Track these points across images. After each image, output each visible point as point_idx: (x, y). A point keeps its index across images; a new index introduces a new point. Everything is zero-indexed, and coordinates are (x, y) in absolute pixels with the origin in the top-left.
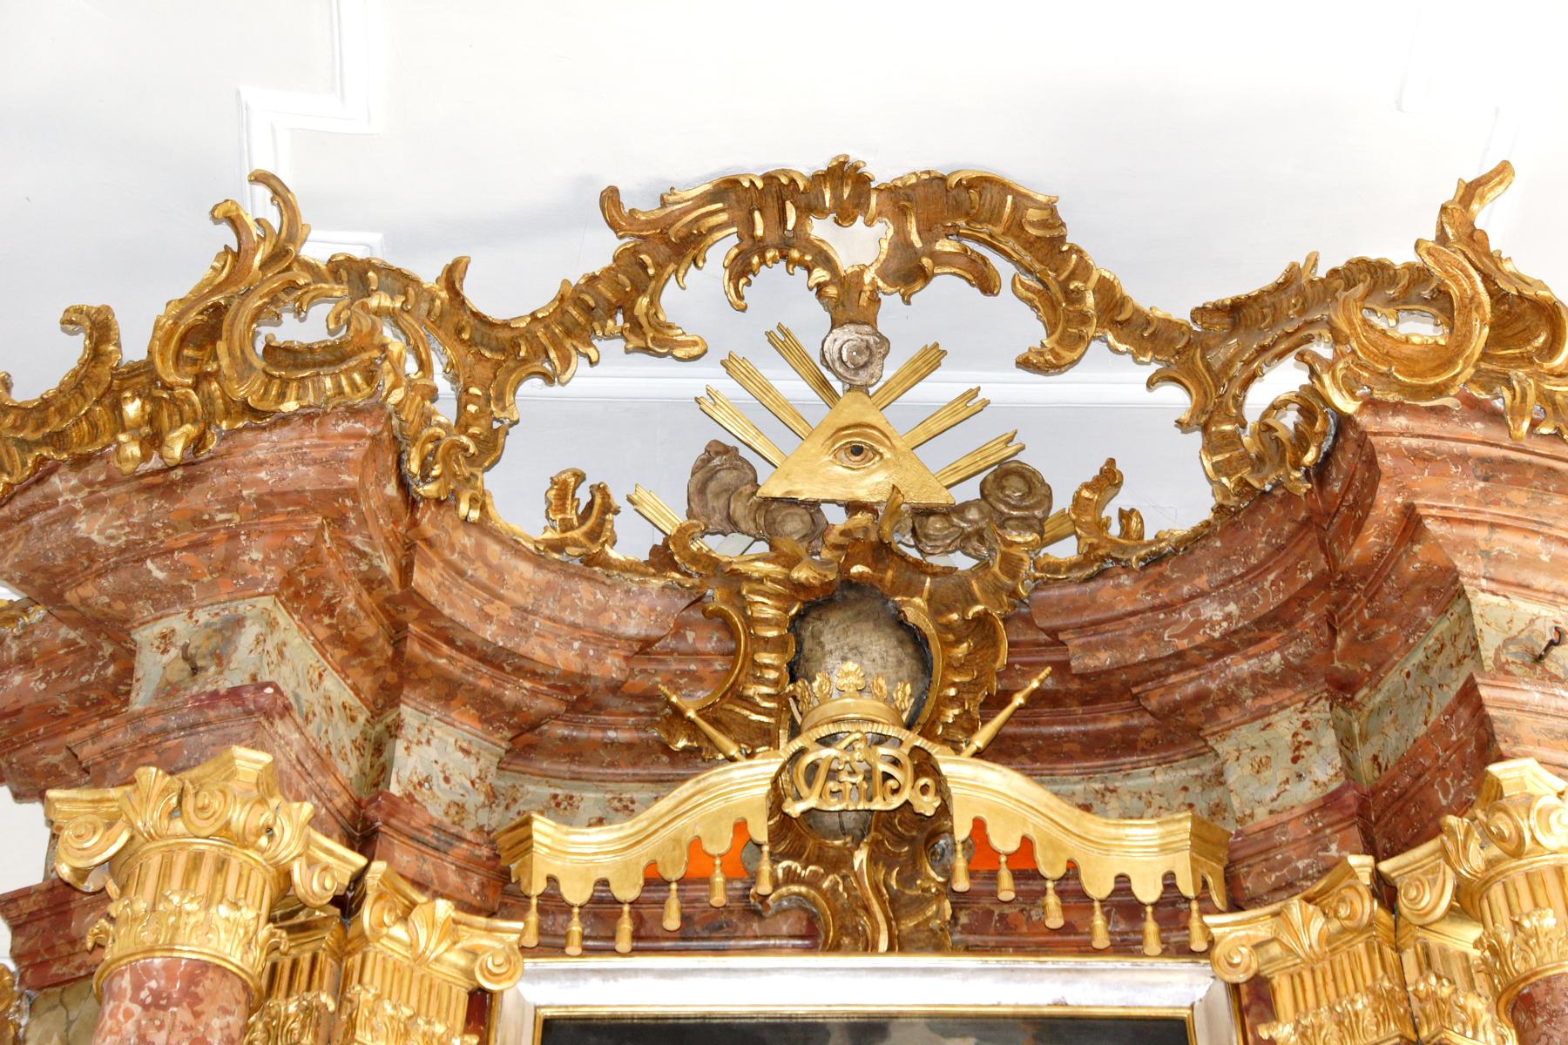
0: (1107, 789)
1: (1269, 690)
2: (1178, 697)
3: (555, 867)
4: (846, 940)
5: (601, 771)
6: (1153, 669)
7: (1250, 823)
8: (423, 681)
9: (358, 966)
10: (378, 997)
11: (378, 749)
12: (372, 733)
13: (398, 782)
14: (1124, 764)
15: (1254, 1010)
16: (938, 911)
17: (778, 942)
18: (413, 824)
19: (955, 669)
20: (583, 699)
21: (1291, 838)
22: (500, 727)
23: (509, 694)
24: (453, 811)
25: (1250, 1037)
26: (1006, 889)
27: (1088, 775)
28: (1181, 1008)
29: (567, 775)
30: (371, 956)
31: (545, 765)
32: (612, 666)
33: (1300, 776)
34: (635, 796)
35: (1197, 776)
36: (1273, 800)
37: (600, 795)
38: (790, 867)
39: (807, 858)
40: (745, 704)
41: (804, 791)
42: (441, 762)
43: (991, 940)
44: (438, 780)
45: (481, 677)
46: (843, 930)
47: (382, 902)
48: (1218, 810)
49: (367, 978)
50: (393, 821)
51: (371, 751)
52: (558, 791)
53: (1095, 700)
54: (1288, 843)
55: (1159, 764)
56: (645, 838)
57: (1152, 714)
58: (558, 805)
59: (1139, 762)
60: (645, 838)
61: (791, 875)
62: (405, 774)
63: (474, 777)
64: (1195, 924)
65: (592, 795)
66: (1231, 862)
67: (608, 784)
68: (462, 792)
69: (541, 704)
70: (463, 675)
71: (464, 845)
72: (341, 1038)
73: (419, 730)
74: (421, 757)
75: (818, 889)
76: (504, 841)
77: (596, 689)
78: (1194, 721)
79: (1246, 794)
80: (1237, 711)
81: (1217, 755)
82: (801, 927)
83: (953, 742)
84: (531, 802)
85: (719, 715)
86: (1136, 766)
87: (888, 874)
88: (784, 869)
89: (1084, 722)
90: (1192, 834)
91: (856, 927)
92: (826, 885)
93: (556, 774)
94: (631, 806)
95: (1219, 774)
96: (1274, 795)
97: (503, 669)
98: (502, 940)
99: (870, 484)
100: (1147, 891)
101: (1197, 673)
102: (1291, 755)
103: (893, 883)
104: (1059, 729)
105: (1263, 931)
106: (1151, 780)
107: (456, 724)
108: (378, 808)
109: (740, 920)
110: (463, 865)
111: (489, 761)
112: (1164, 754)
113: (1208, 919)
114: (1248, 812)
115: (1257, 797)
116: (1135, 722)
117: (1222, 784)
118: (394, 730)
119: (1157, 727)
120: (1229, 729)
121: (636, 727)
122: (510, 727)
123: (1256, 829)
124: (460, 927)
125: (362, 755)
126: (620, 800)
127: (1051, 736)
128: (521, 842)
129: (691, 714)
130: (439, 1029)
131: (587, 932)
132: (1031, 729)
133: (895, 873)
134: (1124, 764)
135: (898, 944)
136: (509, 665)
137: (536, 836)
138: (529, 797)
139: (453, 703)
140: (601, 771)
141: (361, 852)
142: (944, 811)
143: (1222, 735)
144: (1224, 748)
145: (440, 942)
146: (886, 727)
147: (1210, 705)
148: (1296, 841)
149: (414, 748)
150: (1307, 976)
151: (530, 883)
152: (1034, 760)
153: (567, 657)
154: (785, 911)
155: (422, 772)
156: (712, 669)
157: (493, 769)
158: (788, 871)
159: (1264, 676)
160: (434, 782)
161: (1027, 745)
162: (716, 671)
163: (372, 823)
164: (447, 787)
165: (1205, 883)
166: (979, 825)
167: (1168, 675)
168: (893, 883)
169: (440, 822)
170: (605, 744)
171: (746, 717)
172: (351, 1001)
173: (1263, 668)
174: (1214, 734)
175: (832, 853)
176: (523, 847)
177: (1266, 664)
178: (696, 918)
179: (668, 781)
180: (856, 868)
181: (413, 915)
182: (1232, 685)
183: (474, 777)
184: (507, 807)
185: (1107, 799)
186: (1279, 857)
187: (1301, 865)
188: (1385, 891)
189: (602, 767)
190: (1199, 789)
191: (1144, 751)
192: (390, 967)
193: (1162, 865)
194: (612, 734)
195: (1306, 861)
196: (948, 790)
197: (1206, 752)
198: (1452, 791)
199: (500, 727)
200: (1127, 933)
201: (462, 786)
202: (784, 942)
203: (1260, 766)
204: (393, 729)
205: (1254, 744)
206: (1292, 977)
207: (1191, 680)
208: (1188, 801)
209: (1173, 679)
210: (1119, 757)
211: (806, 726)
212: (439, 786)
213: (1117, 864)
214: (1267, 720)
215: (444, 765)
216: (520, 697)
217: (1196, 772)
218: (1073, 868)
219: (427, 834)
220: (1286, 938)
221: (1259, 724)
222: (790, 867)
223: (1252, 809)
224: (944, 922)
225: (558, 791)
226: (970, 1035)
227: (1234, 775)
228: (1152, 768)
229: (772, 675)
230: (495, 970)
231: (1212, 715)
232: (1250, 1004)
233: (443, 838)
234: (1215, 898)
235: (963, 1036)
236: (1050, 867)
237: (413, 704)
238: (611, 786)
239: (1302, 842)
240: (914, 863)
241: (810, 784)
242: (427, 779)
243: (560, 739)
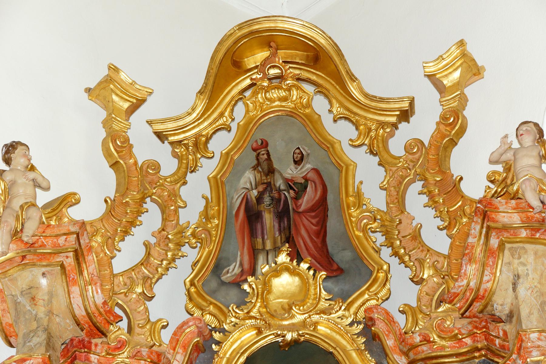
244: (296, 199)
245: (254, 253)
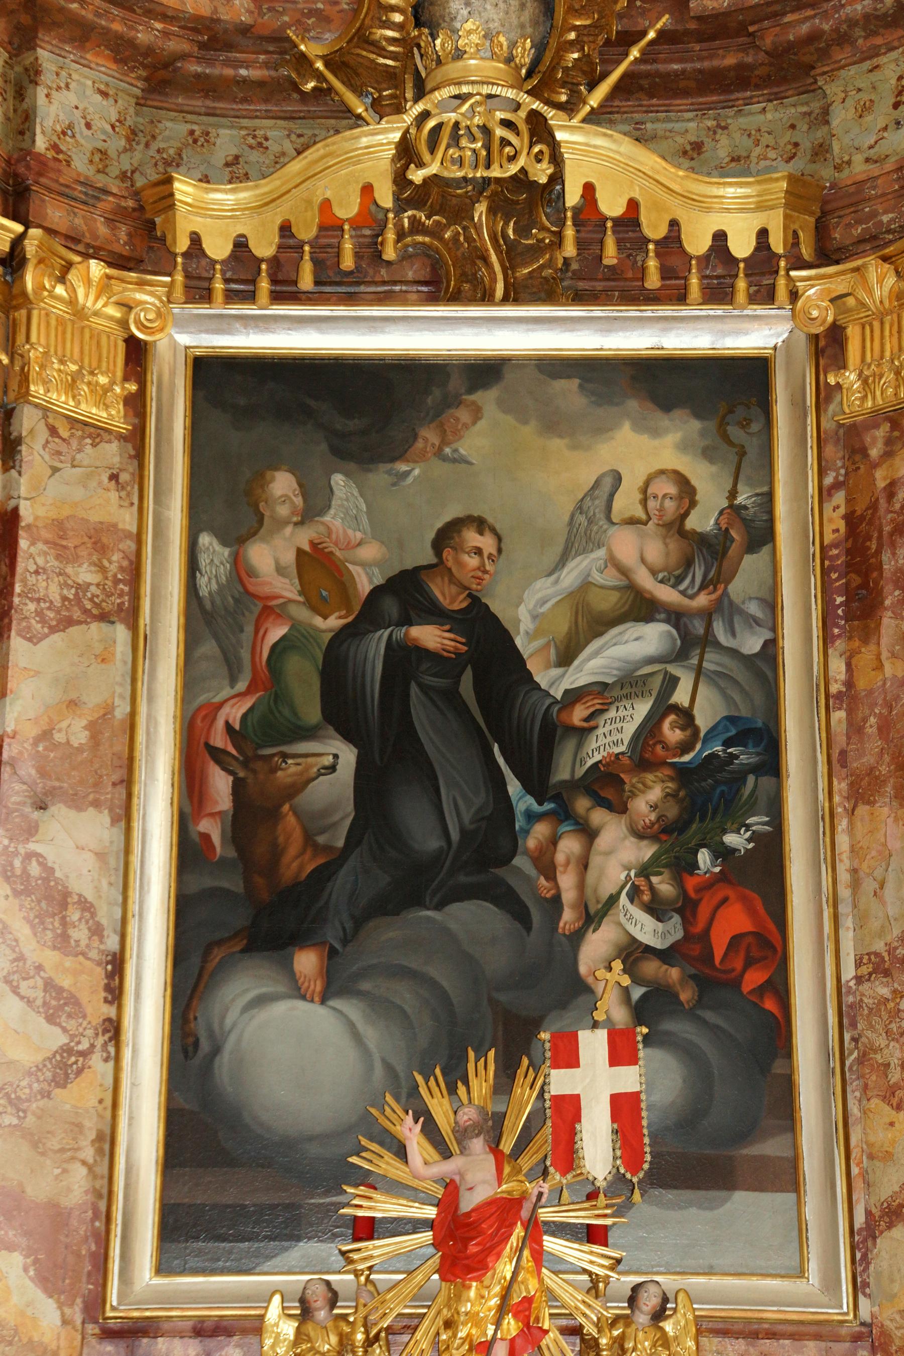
0: (719, 126)
1: (881, 30)
2: (791, 38)
3: (197, 224)
4: (466, 286)
5: (234, 106)
6: (770, 9)
7: (846, 172)
8: (56, 25)
9: (24, 320)
10: (46, 354)
11: (20, 94)
12: (12, 75)
13: (43, 132)
14: (738, 99)
15: (829, 351)
16: (551, 259)
17: (404, 288)
18: (61, 180)
19: (576, 11)
20: (213, 39)
21: (880, 192)
22: (135, 67)
23: (142, 37)
24: (97, 158)
25: (822, 377)
26: (611, 253)
27: (702, 110)
28: (765, 348)
29: (203, 110)
30: (35, 313)
31: (180, 100)
33: (898, 123)
34: (269, 134)
35: (805, 114)
36: (871, 147)
37: (234, 132)
38: (414, 216)
39: (431, 206)
40: (372, 48)
41: (427, 157)
42: (81, 107)
43: (599, 285)
44: (80, 127)
45: (113, 21)
46: (463, 277)
47: (42, 266)
48: (821, 151)
49: (34, 338)
50: (43, 180)
51: (12, 93)
52: (195, 127)
53: (713, 38)
54: (877, 197)
55: (770, 101)
56: (279, 197)
57: (767, 53)
58: (195, 141)
59: (751, 97)
60: (279, 197)
61: (416, 224)
62: (49, 123)
63: (113, 120)
64: (781, 282)
65: (228, 132)
66: (822, 212)
67: (242, 120)
68: (104, 137)
69: (173, 45)
70: (95, 19)
71: (111, 199)
72: (16, 388)
73: (57, 74)
74: (61, 103)
75: (441, 239)
76: (149, 196)
77: (226, 31)
78: (807, 59)
79: (846, 140)
80: (848, 49)
81: (825, 96)
82: (425, 274)
83: (573, 84)
84: (169, 138)
85: (346, 59)
86: (748, 102)
87: (506, 224)
88: (409, 218)
89: (701, 59)
90: (787, 192)
91: (475, 274)
92: (447, 235)
93: (191, 109)
94: (266, 144)
95: (826, 112)
96: (872, 142)
97: (134, 11)
98: (151, 294)
101: (812, 13)
102: (893, 100)
103: (510, 232)
104: (676, 67)
105: (840, 286)
106: (762, 117)
107: (93, 65)
108: (28, 167)
109: (368, 265)
110: (110, 217)
111: (126, 103)
112: (776, 90)
113: (793, 273)
114: (846, 158)
115: (856, 144)
116: (749, 59)
117: (827, 122)
118: (33, 74)
119: (771, 64)
120: (839, 69)
121: (266, 65)
122: (145, 67)
123: (849, 183)
124: (113, 282)
125: (5, 100)
126: (254, 137)
127: (668, 74)
128: (164, 198)
129: (319, 65)
130: (103, 380)
131: (229, 275)
132: (649, 67)
133: (512, 224)
134: (738, 99)
135: (513, 296)
136: (140, 8)
137: (178, 196)
138: (167, 133)
139: (87, 44)
140: (234, 106)
141: (15, 218)
142: (557, 178)
143: (831, 75)
144: (833, 90)
145: (97, 299)
146: (505, 89)
147: (823, 45)
148: (884, 195)
149: (54, 93)
150: (876, 324)
151: (175, 243)
152: (651, 96)
154: (410, 256)
155: (65, 119)
156: (337, 8)
157: (132, 111)
158: (413, 219)
159: (877, 17)
160: (77, 129)
161: (645, 83)
162: (342, 11)
163: (23, 181)
164: (89, 133)
165: (795, 233)
166: (589, 189)
167: (784, 14)
168: (510, 232)
169: (87, 177)
170: (238, 82)
171: (373, 61)
172: (22, 356)
173: (876, 9)
174: (824, 73)
175: (454, 201)
176: (164, 204)
177: (879, 6)
178: (328, 263)
179: (300, 118)
180: (476, 219)
181: (69, 276)
182: (845, 26)
183: (113, 120)
184: (147, 145)
185: (717, 137)
186: (867, 210)
187: (885, 218)
189: (235, 102)
190: (806, 127)
191: (757, 87)
192: (53, 322)
193: (756, 222)
194: (243, 72)
195: (891, 215)
196: (561, 154)
197: (812, 89)
198: (687, 758)
199: (135, 67)
200: (723, 277)
201: (104, 132)
202: (410, 289)
203: (864, 109)
204: (32, 73)
205: (861, 86)
206: (863, 328)
207: (807, 19)
208: (794, 140)
209: (789, 18)
210: (731, 92)
211: (429, 86)
212: (81, 133)
213: (715, 222)
214: (875, 61)
215: (85, 109)
216: (152, 39)
217: (805, 109)
218: (674, 224)
219: (75, 189)
220: (862, 295)
221: (867, 65)
222: (414, 216)
223: (850, 155)
224: (556, 271)
225: (195, 127)
226: (575, 377)
227: (840, 116)
228: (764, 105)
229: (398, 18)
230: (146, 323)
231: (824, 54)
232: (826, 346)
233: (91, 192)
234: (804, 251)
235: (569, 377)
237: (49, 47)
238: (245, 122)
239: (890, 197)
240: (531, 212)
241: (432, 150)
242: (70, 126)
243: (194, 76)
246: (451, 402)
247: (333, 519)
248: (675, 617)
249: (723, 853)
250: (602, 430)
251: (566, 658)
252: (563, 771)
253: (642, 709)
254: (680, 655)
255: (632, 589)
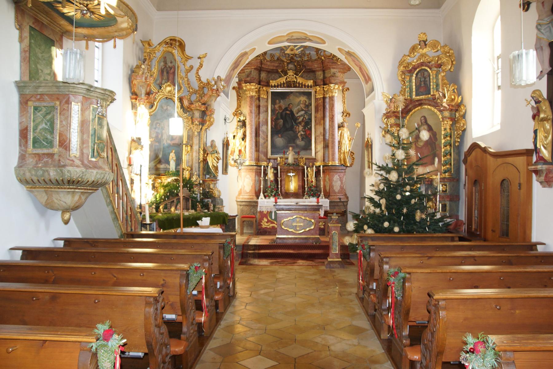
32: (275, 68)
99: (292, 53)
100: (310, 85)
153: (272, 68)
188: (323, 87)
236: (304, 84)
244: (170, 70)
245: (162, 79)
246: (289, 95)
247: (281, 104)
248: (305, 111)
249: (308, 128)
250: (300, 97)
251: (297, 114)
252: (297, 122)
253: (302, 118)
254: (305, 114)
255: (302, 109)
